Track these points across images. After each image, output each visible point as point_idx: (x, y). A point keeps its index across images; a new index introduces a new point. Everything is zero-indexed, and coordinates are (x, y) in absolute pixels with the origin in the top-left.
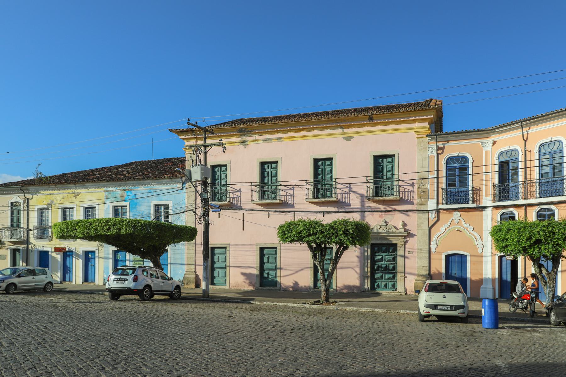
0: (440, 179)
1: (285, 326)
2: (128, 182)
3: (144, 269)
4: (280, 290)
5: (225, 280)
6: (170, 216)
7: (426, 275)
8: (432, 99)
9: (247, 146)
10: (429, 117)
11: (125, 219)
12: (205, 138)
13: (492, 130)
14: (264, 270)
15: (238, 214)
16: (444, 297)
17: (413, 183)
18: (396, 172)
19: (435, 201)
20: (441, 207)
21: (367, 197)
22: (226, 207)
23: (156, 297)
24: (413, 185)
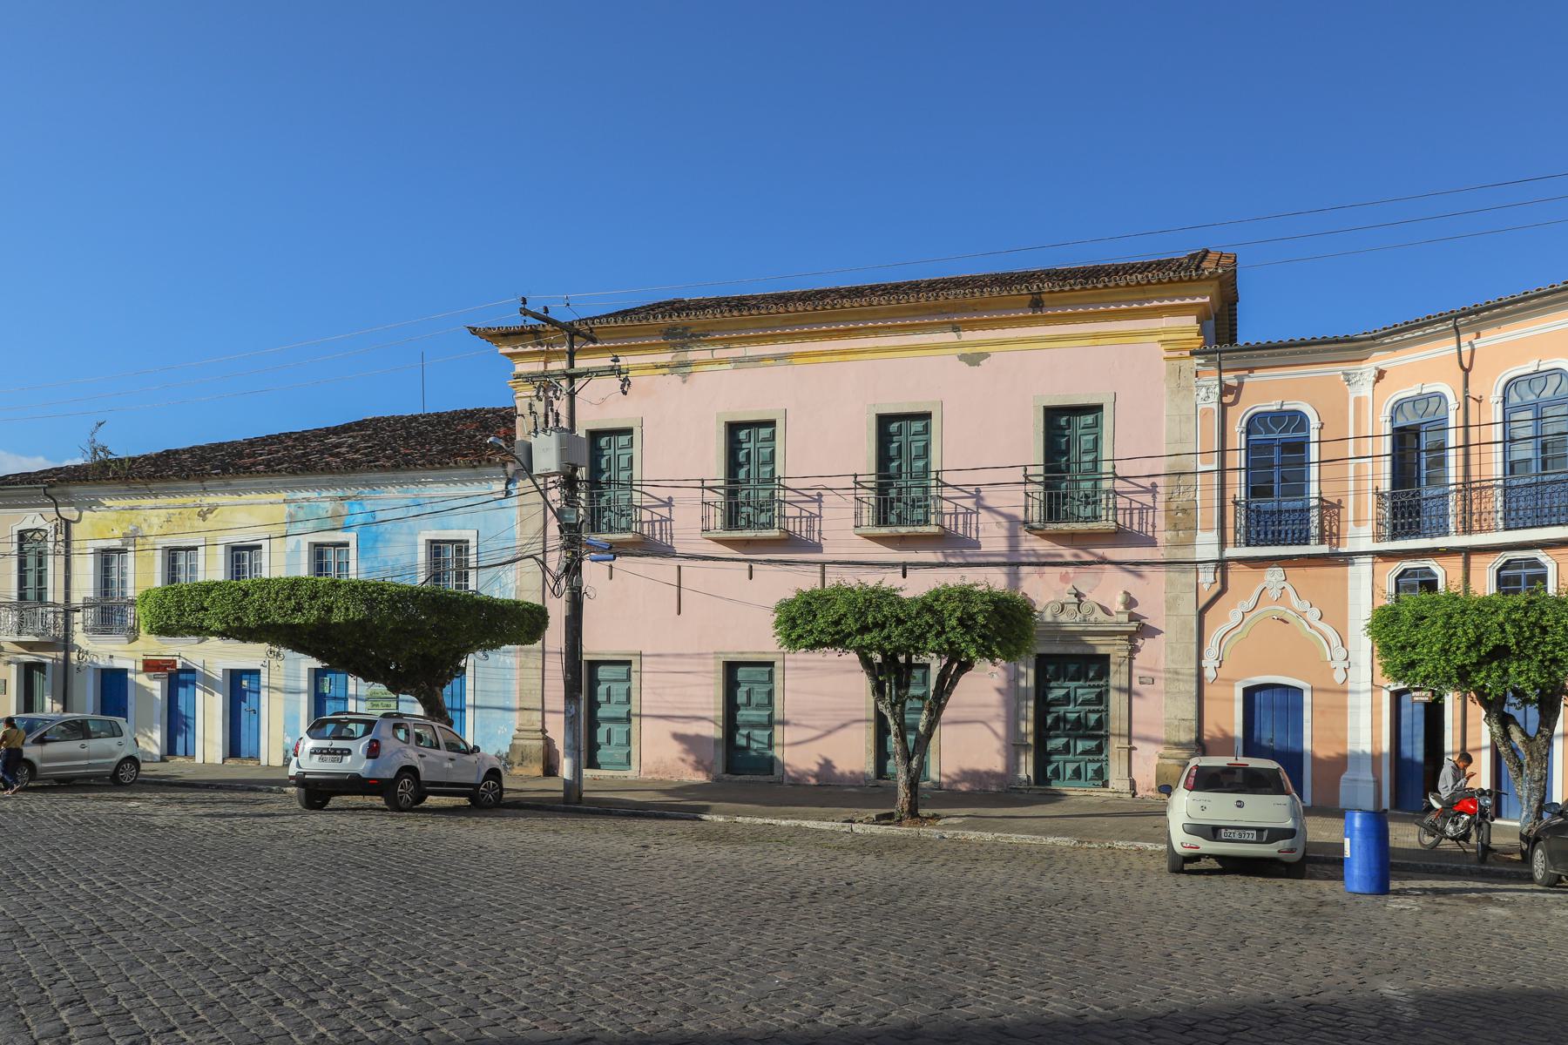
0: (1229, 475)
1: (794, 883)
2: (352, 476)
3: (397, 721)
4: (781, 783)
5: (629, 755)
6: (472, 574)
7: (1190, 743)
8: (1207, 252)
9: (689, 378)
10: (1199, 300)
11: (344, 579)
12: (572, 355)
13: (1373, 338)
14: (737, 728)
15: (664, 569)
16: (1240, 804)
17: (1154, 486)
18: (1106, 453)
19: (1214, 536)
20: (1231, 552)
21: (1025, 523)
22: (631, 550)
23: (431, 801)
24: (1153, 490)
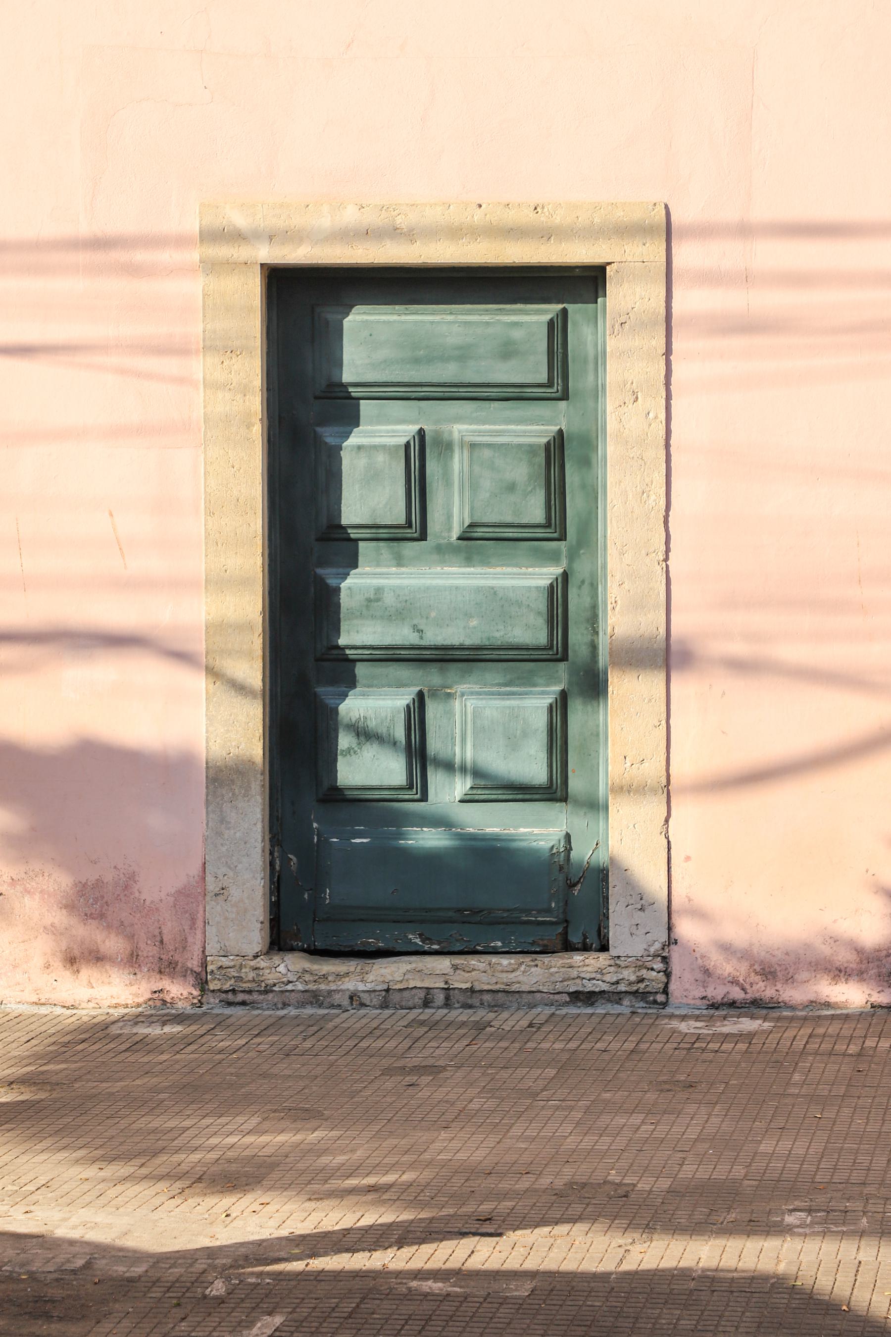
4: (652, 998)
14: (341, 669)
